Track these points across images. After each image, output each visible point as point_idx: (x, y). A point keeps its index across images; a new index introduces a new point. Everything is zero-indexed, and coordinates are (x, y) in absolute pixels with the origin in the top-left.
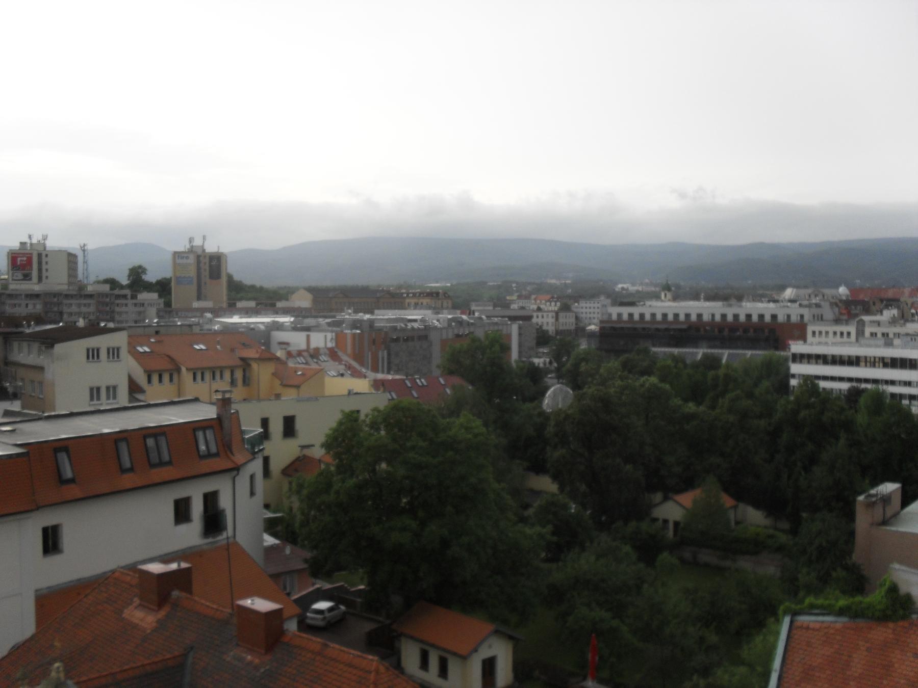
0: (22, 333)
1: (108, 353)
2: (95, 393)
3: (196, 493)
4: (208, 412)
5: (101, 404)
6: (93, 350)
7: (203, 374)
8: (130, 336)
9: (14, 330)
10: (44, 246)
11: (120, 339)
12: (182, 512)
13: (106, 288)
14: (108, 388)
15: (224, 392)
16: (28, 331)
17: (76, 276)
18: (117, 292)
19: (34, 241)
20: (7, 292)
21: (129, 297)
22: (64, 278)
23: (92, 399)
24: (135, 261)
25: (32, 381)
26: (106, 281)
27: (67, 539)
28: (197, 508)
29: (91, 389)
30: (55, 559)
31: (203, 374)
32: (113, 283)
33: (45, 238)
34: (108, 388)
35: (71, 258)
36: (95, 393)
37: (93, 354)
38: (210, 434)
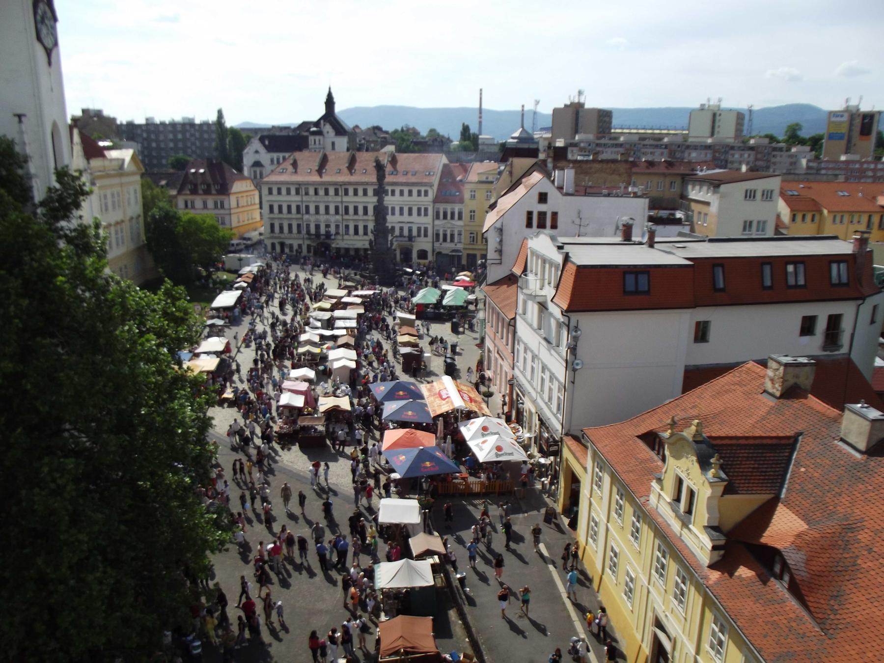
0: (696, 175)
1: (763, 195)
2: (747, 225)
3: (822, 312)
4: (844, 247)
5: (751, 234)
6: (751, 191)
7: (842, 217)
8: (783, 181)
9: (691, 172)
10: (719, 106)
11: (774, 184)
12: (808, 326)
13: (767, 141)
14: (759, 222)
15: (863, 233)
16: (700, 174)
17: (742, 131)
18: (774, 145)
19: (712, 103)
20: (687, 144)
21: (784, 149)
22: (732, 133)
23: (744, 229)
24: (793, 120)
25: (700, 213)
26: (767, 136)
27: (713, 333)
28: (821, 325)
29: (745, 222)
30: (703, 345)
31: (842, 217)
32: (772, 138)
33: (720, 100)
34: (759, 222)
35: (740, 116)
36: (747, 225)
37: (750, 195)
38: (843, 266)
